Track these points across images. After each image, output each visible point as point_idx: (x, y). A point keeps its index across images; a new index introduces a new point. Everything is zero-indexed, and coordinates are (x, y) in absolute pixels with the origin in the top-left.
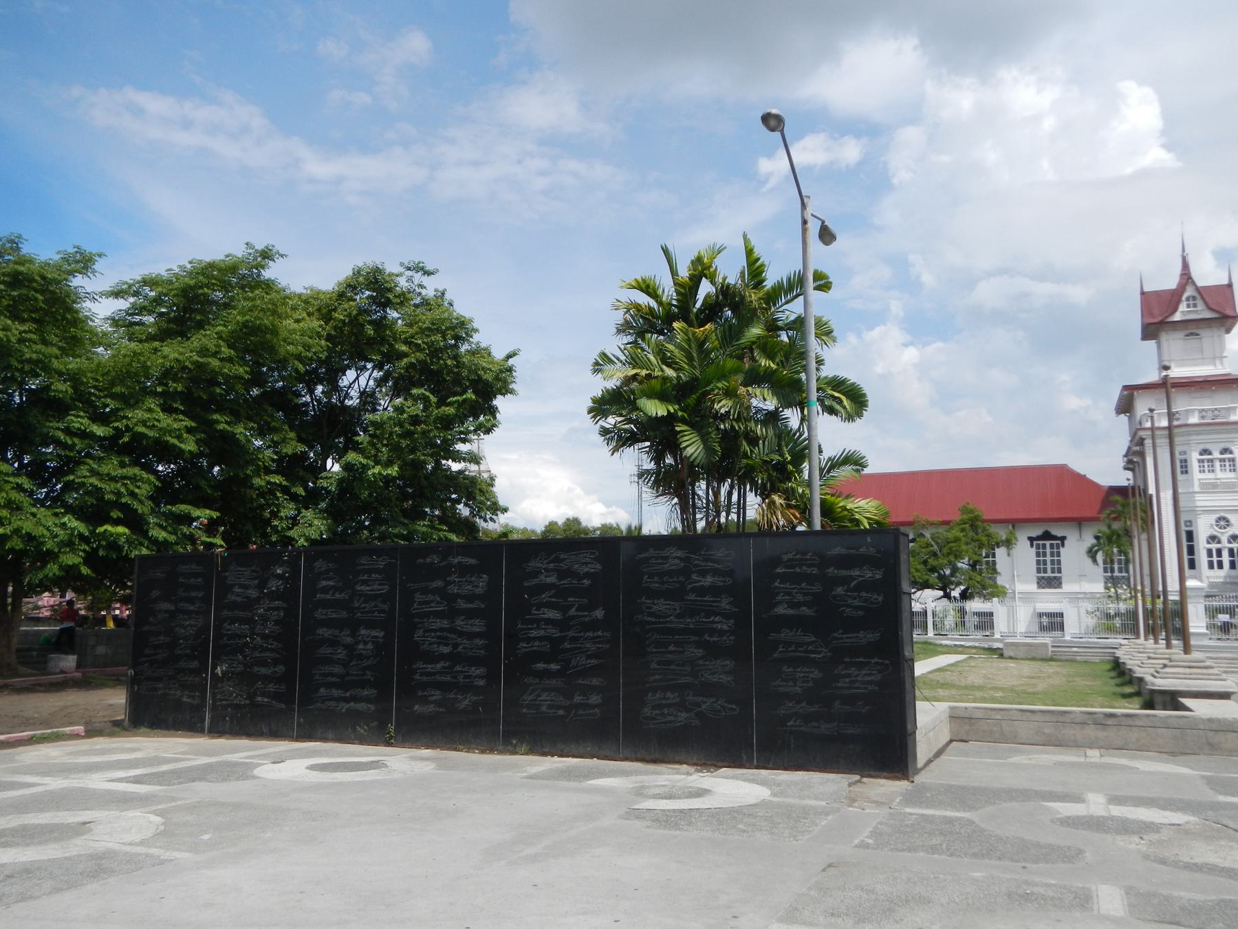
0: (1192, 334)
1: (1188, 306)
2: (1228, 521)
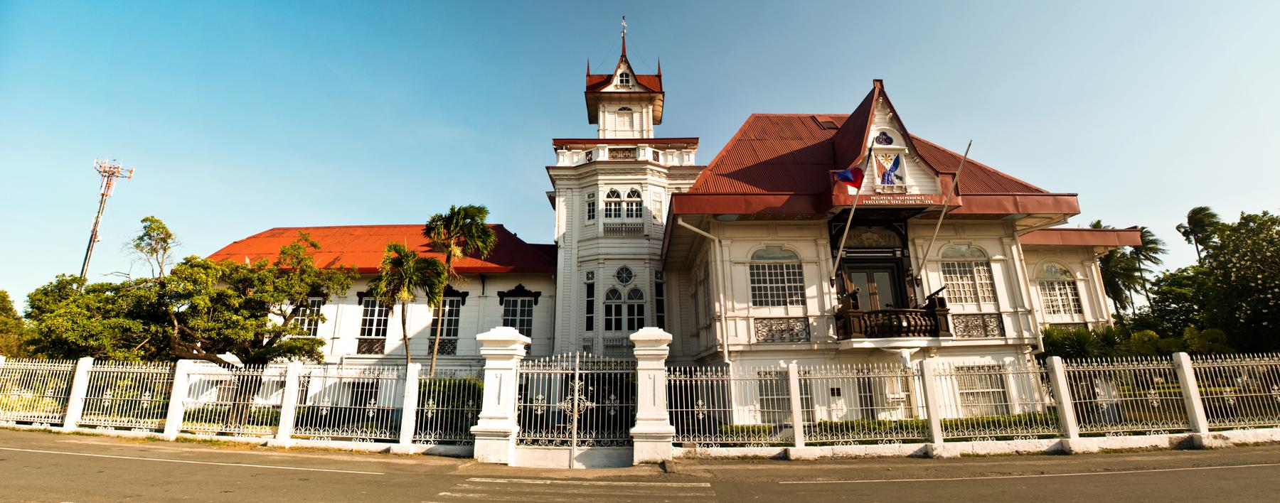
0: (624, 109)
1: (622, 81)
2: (630, 273)
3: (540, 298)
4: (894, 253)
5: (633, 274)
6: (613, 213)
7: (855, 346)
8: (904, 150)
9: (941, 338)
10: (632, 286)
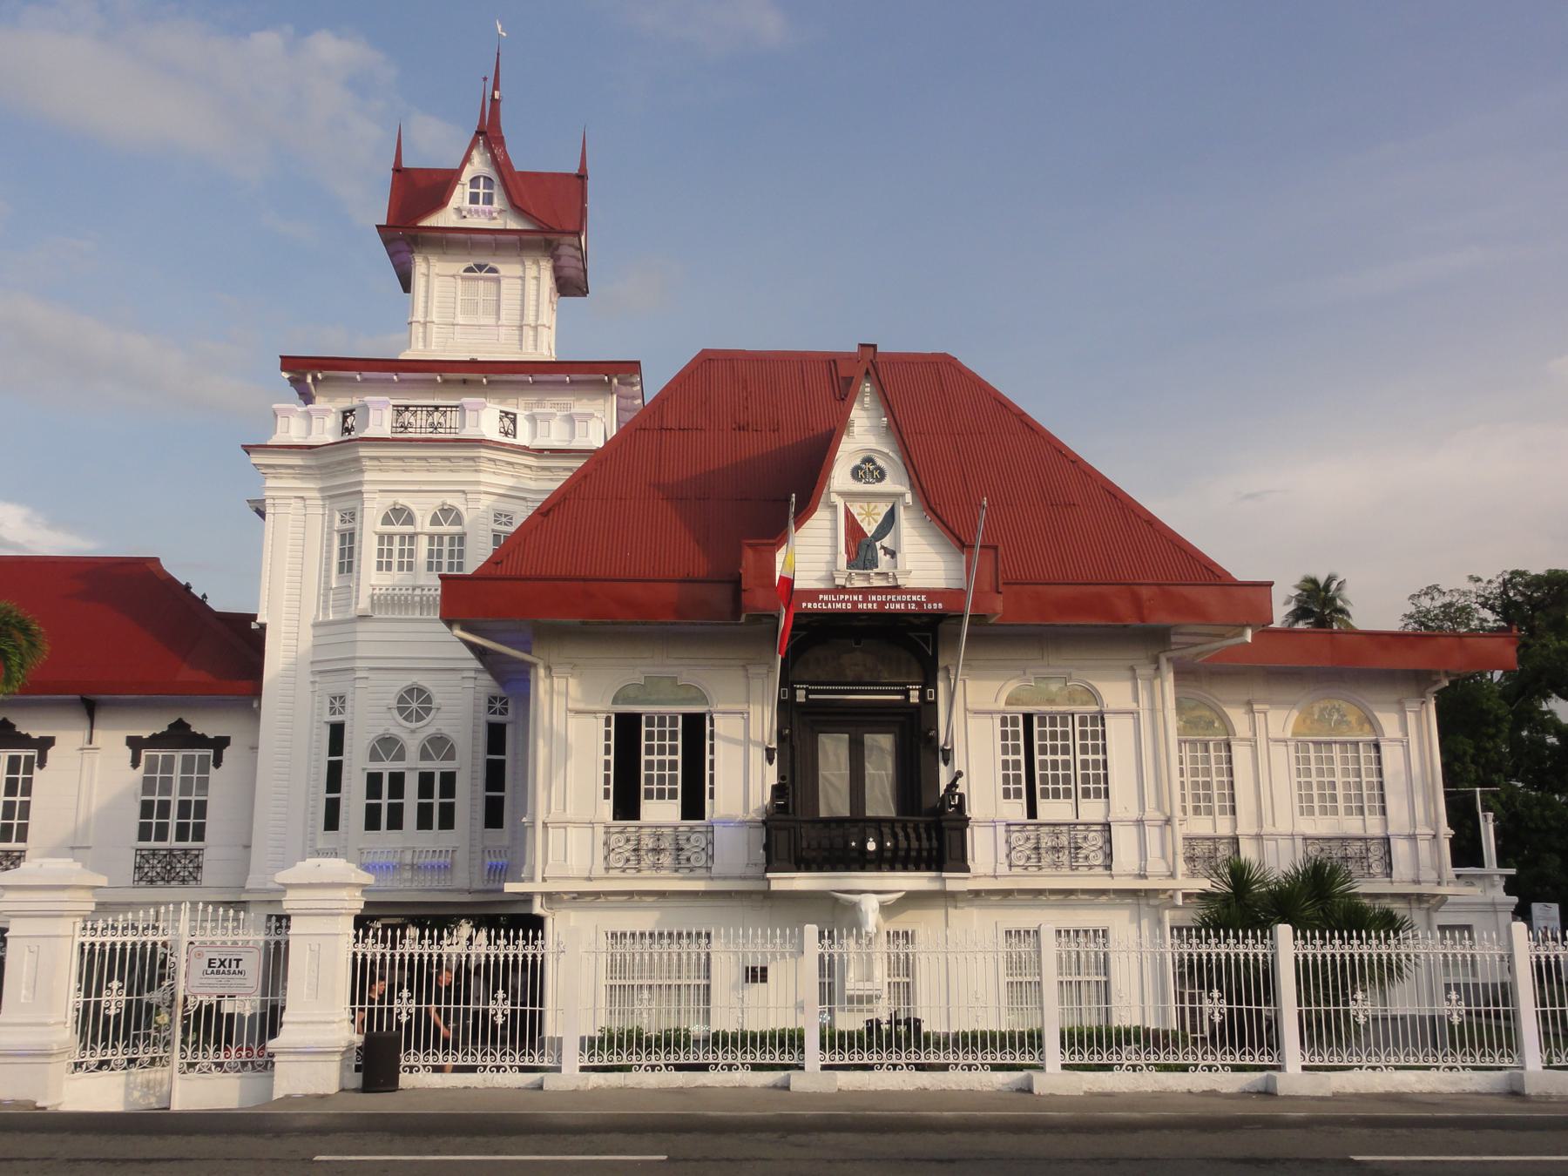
0: (480, 268)
1: (474, 199)
2: (429, 700)
3: (226, 752)
4: (906, 693)
5: (436, 702)
6: (395, 559)
7: (776, 886)
8: (903, 495)
9: (945, 874)
10: (431, 730)
